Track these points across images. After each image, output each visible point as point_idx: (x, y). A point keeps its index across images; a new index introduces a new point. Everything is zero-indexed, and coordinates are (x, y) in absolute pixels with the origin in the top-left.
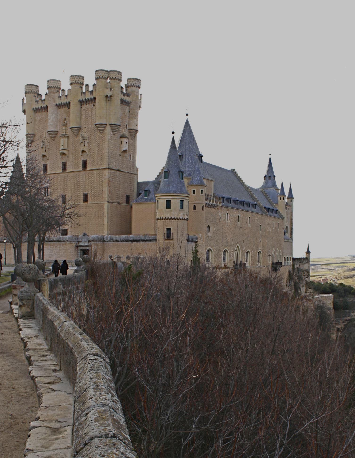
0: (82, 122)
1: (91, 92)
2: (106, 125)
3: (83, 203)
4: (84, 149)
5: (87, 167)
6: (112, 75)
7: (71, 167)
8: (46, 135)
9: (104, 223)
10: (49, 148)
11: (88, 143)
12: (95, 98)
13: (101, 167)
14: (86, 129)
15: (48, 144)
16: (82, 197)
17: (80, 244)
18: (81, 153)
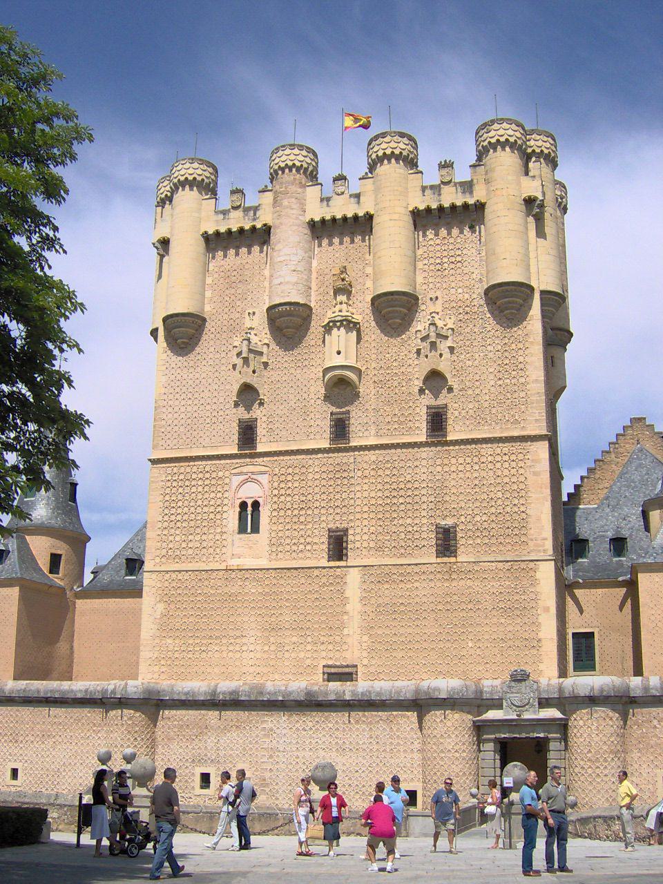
0: (419, 279)
1: (468, 187)
2: (532, 289)
3: (434, 560)
4: (443, 366)
5: (449, 428)
6: (540, 143)
7: (373, 430)
8: (259, 322)
9: (541, 635)
10: (266, 365)
11: (452, 349)
12: (480, 207)
13: (516, 433)
14: (439, 302)
15: (265, 349)
16: (431, 539)
17: (492, 715)
18: (419, 383)
